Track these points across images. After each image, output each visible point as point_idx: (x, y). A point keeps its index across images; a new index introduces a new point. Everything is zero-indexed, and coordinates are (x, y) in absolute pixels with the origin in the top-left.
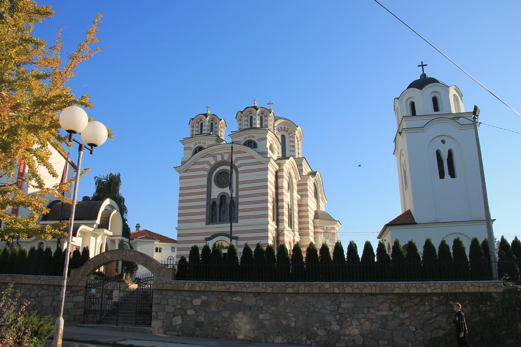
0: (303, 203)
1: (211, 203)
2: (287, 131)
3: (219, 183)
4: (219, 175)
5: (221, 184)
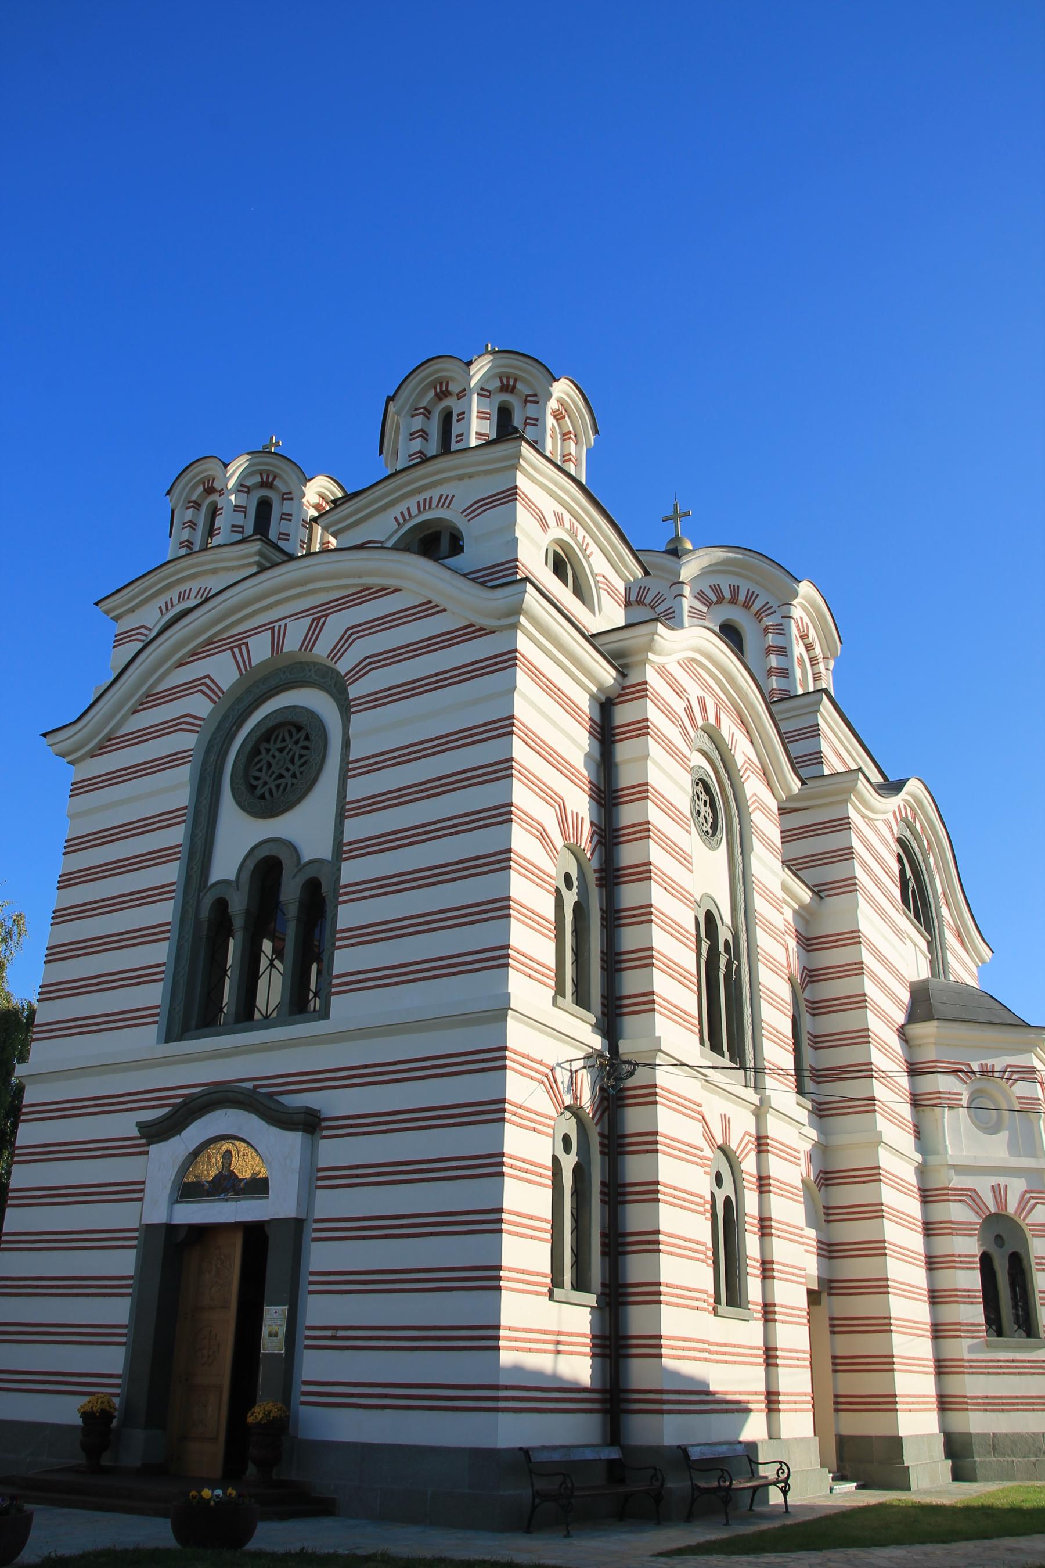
0: (830, 927)
1: (205, 913)
2: (747, 605)
3: (259, 792)
4: (263, 747)
5: (267, 795)
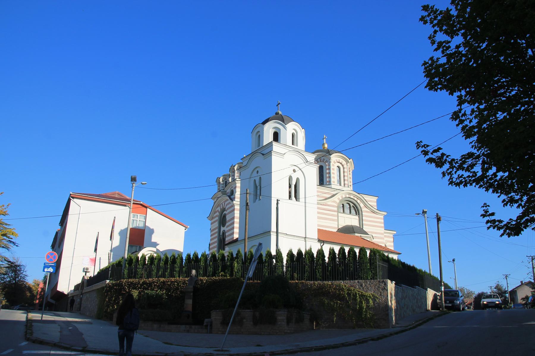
2: (323, 161)
